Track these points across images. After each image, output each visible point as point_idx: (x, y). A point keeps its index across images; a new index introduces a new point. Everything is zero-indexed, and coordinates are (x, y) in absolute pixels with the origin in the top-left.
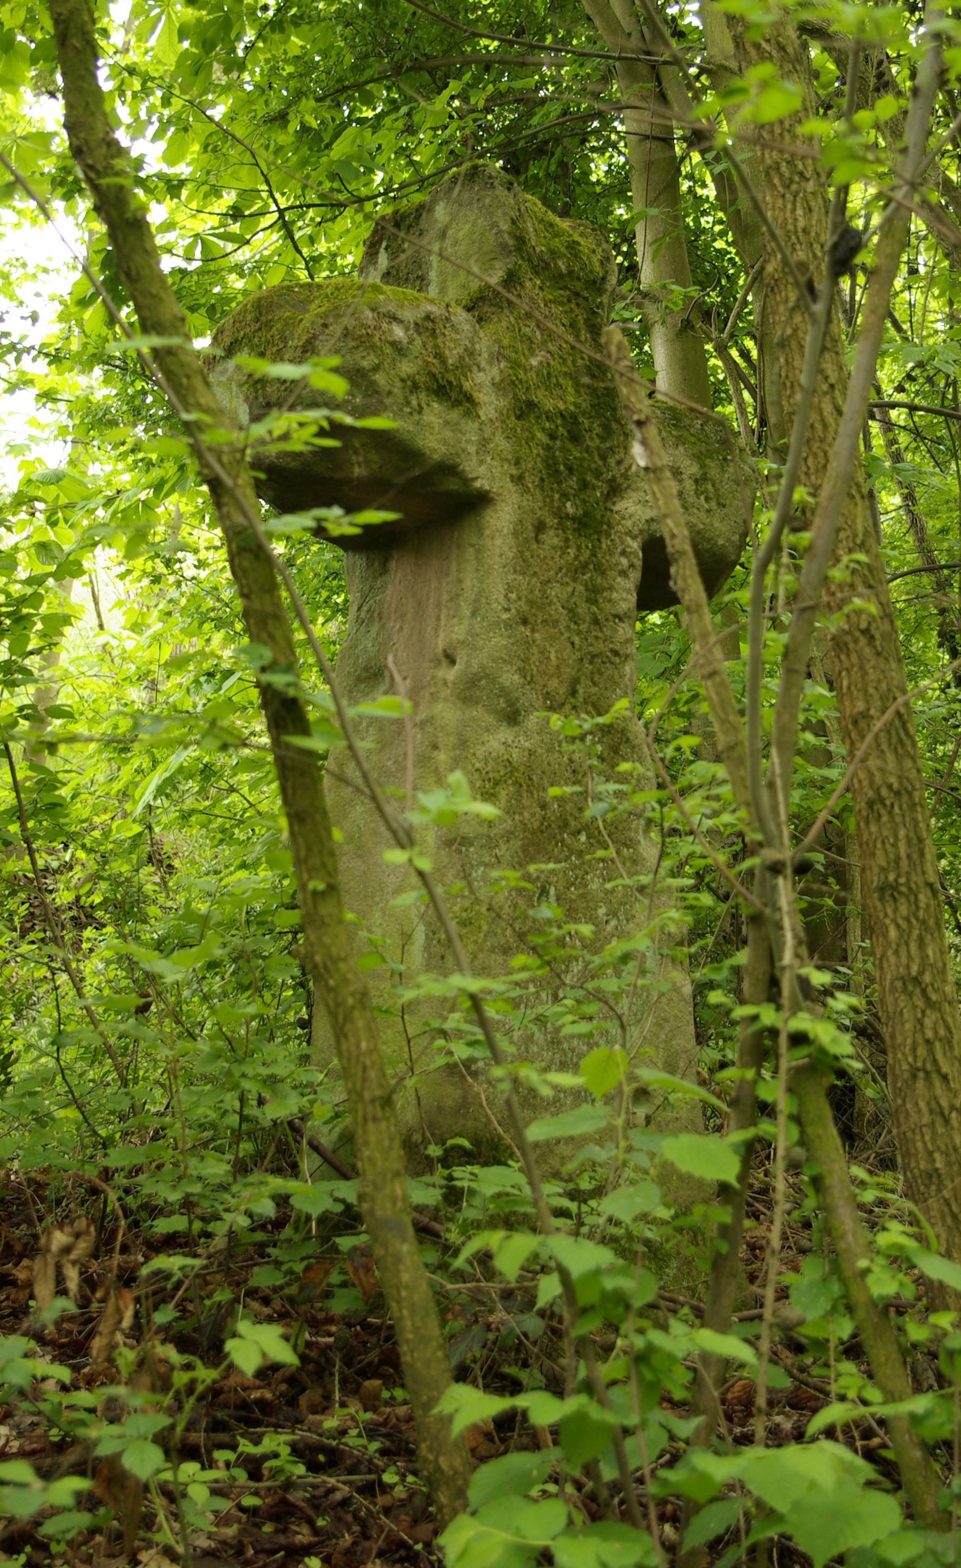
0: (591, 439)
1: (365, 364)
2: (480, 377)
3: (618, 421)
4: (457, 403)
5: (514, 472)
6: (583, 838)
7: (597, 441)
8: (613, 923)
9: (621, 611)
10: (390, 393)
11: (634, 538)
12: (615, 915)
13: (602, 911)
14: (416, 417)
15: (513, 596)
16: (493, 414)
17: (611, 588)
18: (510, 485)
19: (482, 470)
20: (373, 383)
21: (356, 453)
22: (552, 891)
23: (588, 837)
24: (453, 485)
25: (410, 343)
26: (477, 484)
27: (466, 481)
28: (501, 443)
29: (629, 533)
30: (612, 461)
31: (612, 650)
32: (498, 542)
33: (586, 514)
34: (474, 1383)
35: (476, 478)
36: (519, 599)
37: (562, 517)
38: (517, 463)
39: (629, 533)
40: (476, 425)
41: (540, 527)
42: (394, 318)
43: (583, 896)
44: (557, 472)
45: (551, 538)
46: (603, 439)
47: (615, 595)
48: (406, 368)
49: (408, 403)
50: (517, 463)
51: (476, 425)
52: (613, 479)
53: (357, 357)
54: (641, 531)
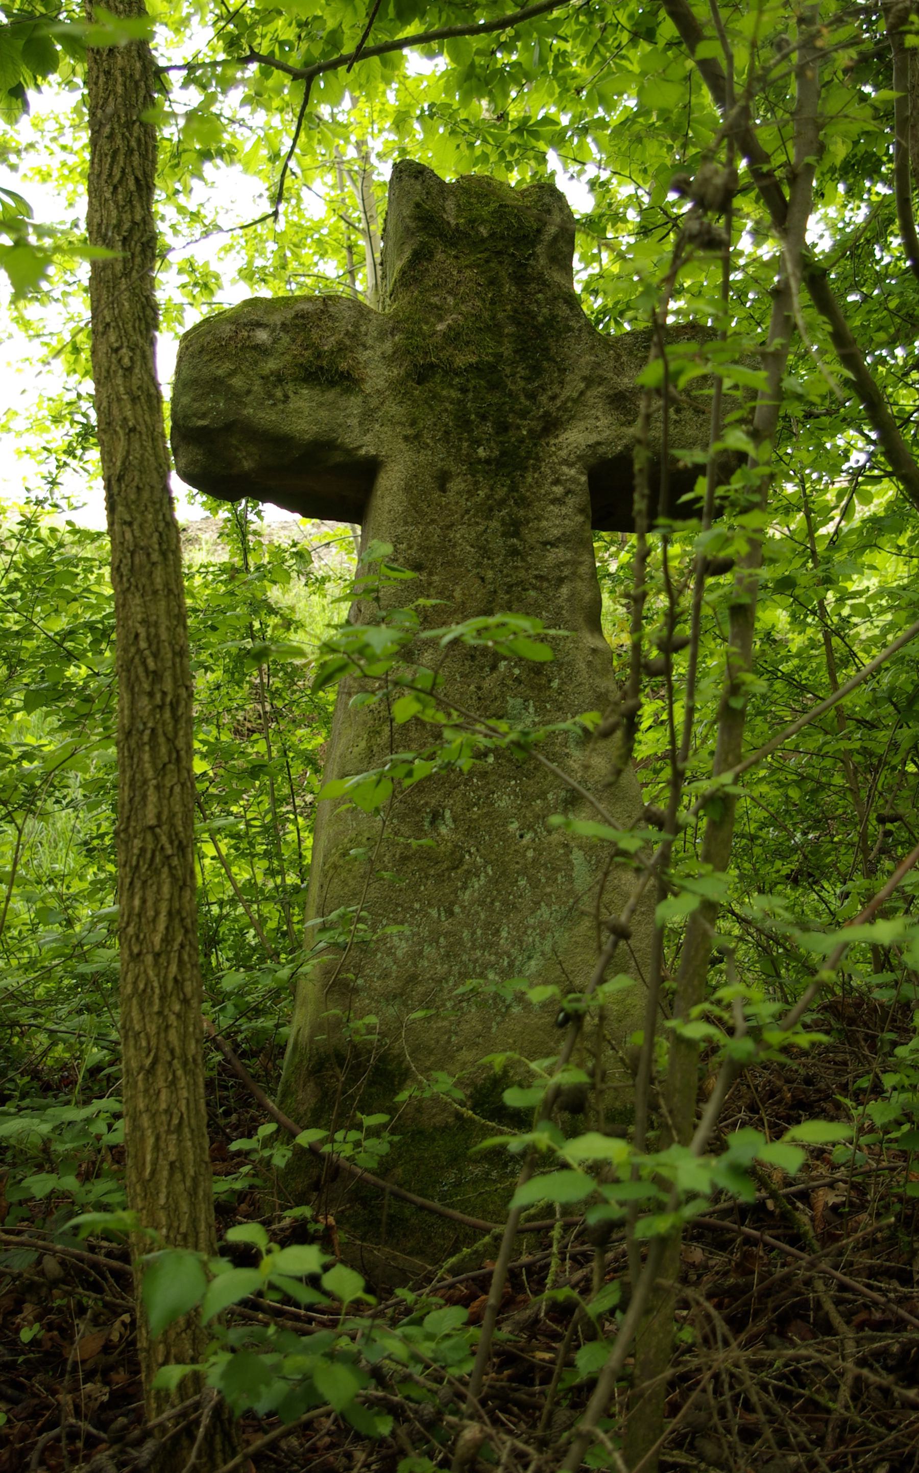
0: (514, 383)
1: (220, 372)
2: (364, 355)
3: (551, 360)
4: (332, 384)
5: (410, 432)
6: (491, 759)
7: (522, 383)
8: (529, 836)
9: (551, 538)
10: (249, 392)
11: (571, 465)
12: (530, 827)
13: (514, 827)
14: (281, 406)
15: (403, 546)
16: (381, 384)
17: (539, 518)
18: (403, 446)
19: (368, 438)
20: (230, 387)
21: (238, 449)
22: (448, 814)
23: (496, 758)
24: (338, 458)
25: (274, 342)
26: (363, 452)
27: (349, 452)
28: (393, 409)
29: (565, 462)
30: (544, 399)
31: (536, 577)
32: (388, 500)
33: (503, 453)
34: (579, 1202)
35: (360, 447)
36: (410, 548)
37: (473, 464)
38: (413, 424)
39: (565, 462)
40: (360, 399)
41: (442, 480)
42: (259, 325)
43: (487, 814)
44: (468, 422)
45: (456, 485)
46: (528, 380)
47: (544, 523)
48: (272, 365)
49: (270, 396)
50: (413, 424)
51: (360, 399)
52: (547, 414)
53: (213, 367)
54: (579, 458)
